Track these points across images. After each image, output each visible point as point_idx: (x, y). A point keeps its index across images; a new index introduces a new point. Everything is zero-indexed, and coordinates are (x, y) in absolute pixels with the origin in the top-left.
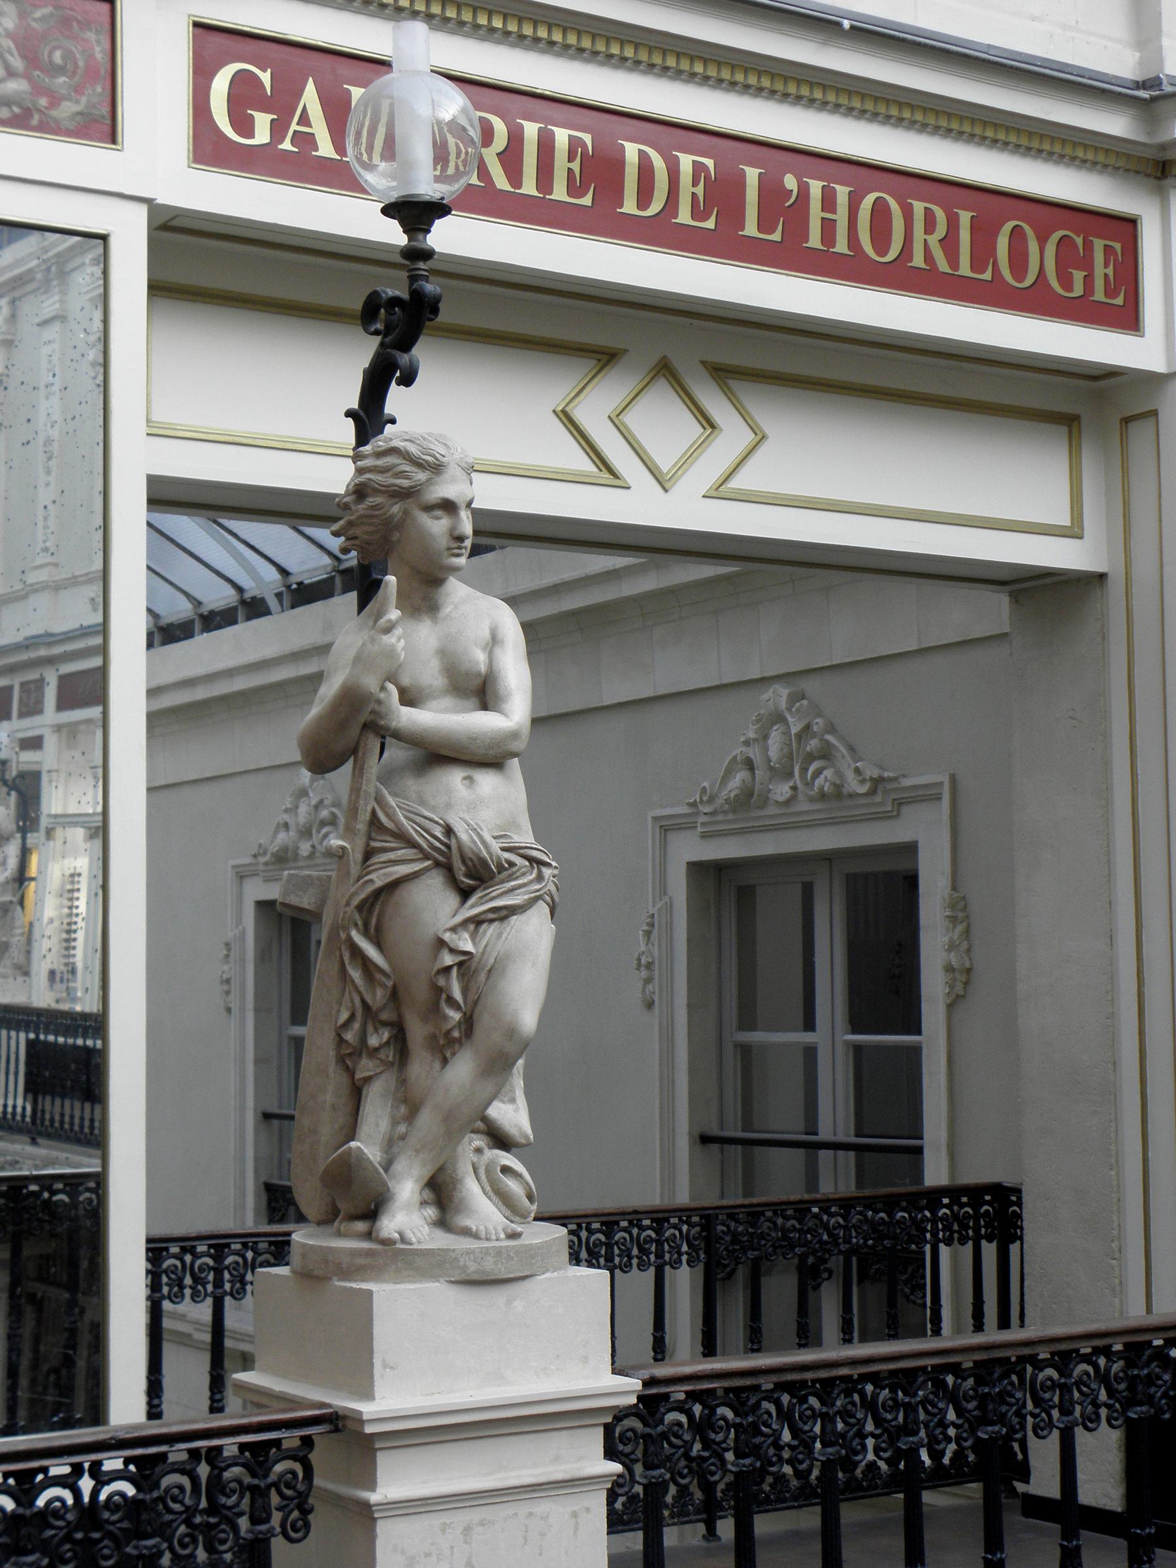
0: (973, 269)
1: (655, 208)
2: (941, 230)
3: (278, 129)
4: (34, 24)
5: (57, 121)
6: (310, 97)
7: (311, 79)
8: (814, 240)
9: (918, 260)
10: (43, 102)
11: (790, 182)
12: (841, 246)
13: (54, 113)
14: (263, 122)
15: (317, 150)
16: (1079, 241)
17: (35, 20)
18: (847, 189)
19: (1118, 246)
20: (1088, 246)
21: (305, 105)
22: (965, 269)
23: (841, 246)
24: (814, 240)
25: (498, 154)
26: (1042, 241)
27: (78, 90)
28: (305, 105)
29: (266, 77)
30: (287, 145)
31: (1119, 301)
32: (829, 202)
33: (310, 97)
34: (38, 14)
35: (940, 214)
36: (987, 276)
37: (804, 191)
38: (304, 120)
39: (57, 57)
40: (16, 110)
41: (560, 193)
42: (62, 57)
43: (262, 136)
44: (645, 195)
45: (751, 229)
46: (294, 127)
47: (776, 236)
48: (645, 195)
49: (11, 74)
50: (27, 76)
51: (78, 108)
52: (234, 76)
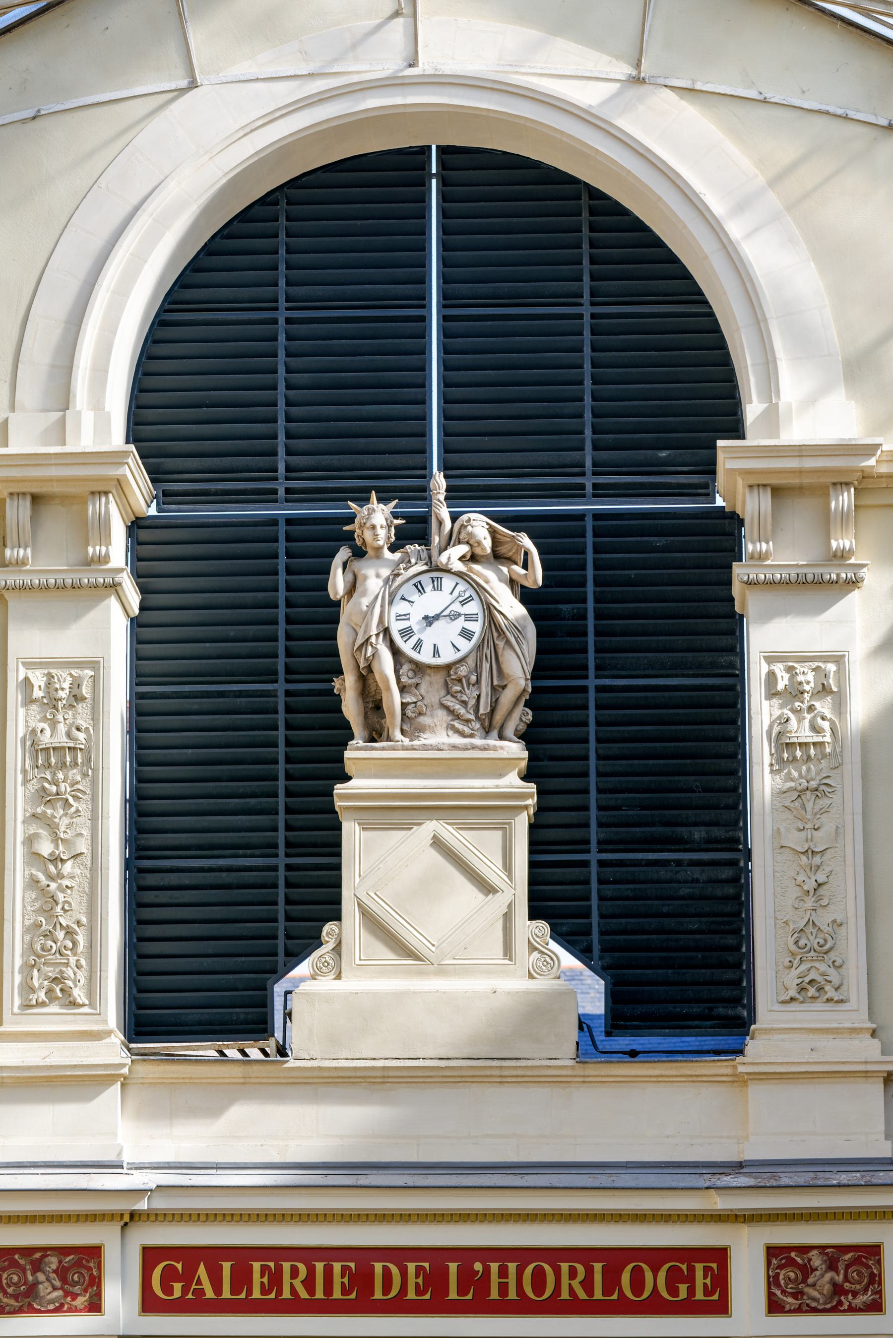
0: (604, 1295)
1: (393, 1294)
2: (581, 1275)
3: (185, 1290)
4: (65, 1264)
5: (76, 1307)
6: (202, 1271)
7: (202, 1263)
8: (494, 1294)
9: (565, 1295)
10: (69, 1299)
11: (478, 1266)
12: (512, 1295)
13: (74, 1303)
14: (178, 1287)
15: (205, 1295)
16: (684, 1267)
17: (66, 1263)
18: (515, 1264)
19: (714, 1266)
20: (691, 1270)
21: (199, 1276)
22: (598, 1295)
23: (512, 1295)
24: (494, 1294)
25: (301, 1282)
26: (655, 1272)
27: (85, 1291)
28: (199, 1276)
29: (179, 1266)
30: (190, 1296)
31: (716, 1297)
32: (503, 1273)
33: (202, 1271)
34: (67, 1260)
35: (580, 1268)
36: (615, 1297)
37: (487, 1270)
38: (199, 1282)
39: (76, 1277)
40: (57, 1304)
41: (337, 1294)
42: (78, 1277)
43: (177, 1293)
44: (387, 1289)
45: (453, 1295)
46: (194, 1287)
47: (470, 1296)
48: (387, 1289)
49: (55, 1288)
50: (62, 1288)
51: (85, 1299)
52: (163, 1268)
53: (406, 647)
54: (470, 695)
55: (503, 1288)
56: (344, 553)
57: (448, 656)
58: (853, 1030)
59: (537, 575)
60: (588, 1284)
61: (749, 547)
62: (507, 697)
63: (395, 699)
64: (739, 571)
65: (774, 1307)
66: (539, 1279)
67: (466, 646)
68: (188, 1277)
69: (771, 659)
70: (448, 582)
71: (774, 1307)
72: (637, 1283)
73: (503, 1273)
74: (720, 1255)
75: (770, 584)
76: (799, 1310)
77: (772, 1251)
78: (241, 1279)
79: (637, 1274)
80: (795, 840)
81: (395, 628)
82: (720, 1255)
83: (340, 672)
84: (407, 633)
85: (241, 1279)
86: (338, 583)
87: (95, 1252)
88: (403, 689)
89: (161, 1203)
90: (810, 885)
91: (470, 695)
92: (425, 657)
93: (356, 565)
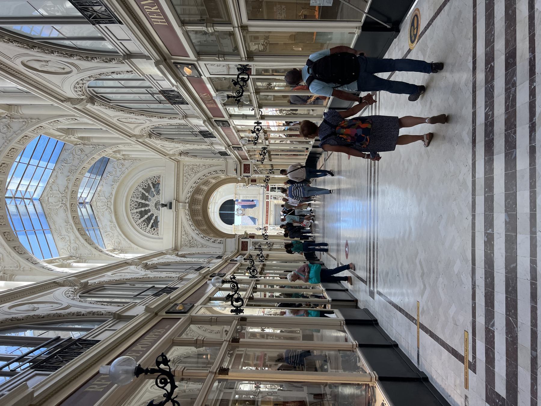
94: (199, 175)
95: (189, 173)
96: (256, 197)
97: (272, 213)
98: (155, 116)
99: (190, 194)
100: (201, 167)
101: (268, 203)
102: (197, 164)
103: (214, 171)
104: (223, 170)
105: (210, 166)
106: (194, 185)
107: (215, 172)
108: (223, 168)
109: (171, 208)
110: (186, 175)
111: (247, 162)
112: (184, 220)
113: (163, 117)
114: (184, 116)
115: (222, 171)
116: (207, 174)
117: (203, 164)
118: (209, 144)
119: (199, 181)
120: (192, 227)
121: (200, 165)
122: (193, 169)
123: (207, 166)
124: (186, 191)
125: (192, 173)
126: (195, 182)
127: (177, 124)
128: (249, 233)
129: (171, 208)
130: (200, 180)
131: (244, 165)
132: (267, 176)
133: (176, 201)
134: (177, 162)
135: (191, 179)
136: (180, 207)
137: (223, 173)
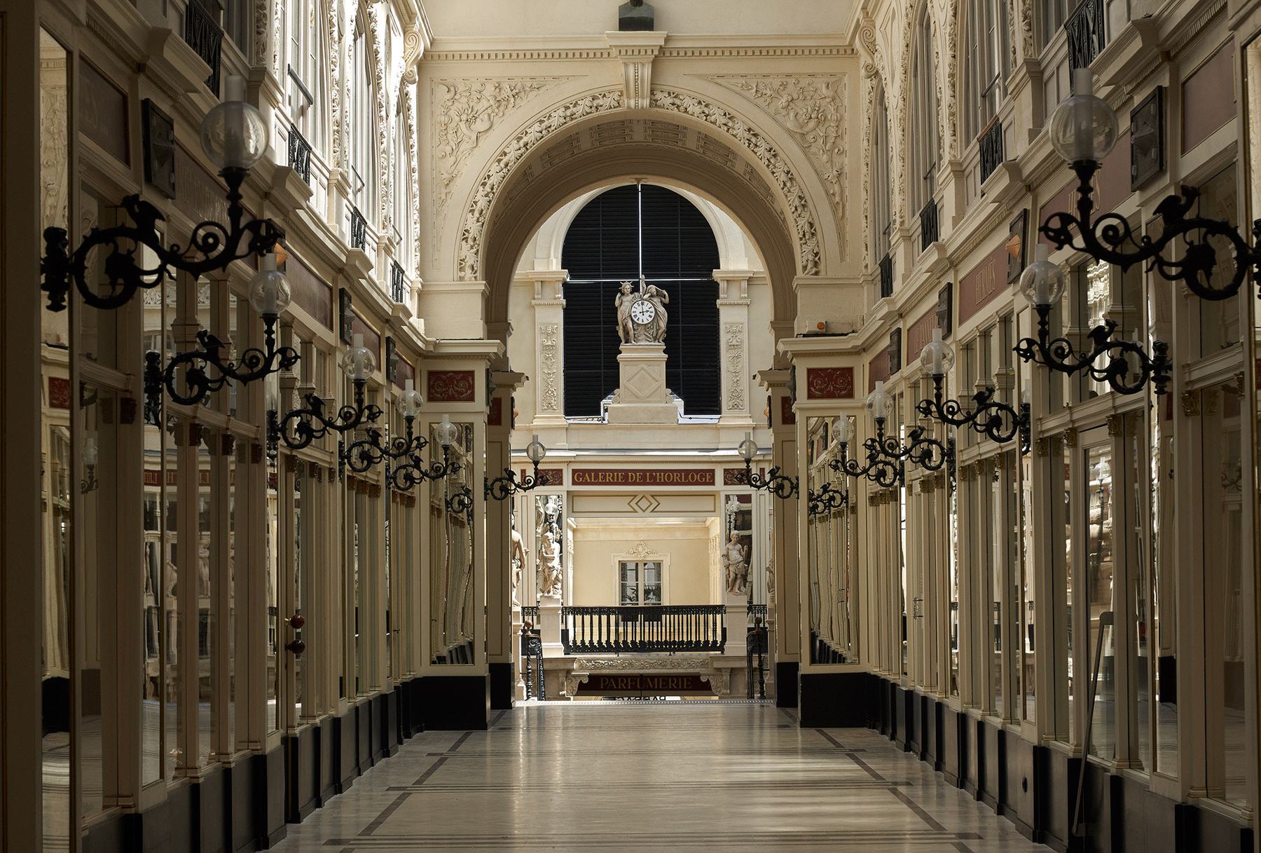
32: (660, 475)
53: (635, 320)
54: (651, 332)
55: (660, 479)
56: (619, 295)
57: (646, 322)
58: (746, 417)
59: (667, 300)
60: (681, 478)
61: (721, 296)
62: (660, 331)
63: (632, 333)
64: (718, 302)
65: (726, 484)
66: (669, 479)
67: (650, 319)
68: (583, 476)
69: (726, 324)
70: (646, 303)
71: (726, 484)
72: (693, 478)
73: (660, 475)
74: (713, 471)
75: (726, 305)
76: (731, 484)
77: (725, 470)
78: (596, 477)
79: (693, 476)
80: (731, 369)
81: (633, 314)
82: (713, 471)
83: (618, 325)
84: (635, 316)
85: (596, 477)
86: (617, 303)
87: (561, 470)
88: (634, 330)
89: (577, 459)
90: (735, 380)
91: (651, 332)
92: (640, 322)
93: (622, 298)
94: (791, 151)
95: (799, 103)
96: (735, 406)
97: (644, 504)
98: (954, 57)
99: (697, 110)
100: (831, 161)
101: (706, 477)
102: (846, 138)
103: (811, 225)
104: (822, 267)
105: (838, 208)
106: (740, 130)
107: (807, 228)
108: (831, 268)
109: (626, 24)
110: (791, 87)
111: (861, 380)
112: (569, 90)
113: (954, 86)
114: (961, 164)
115: (816, 264)
116: (796, 191)
117: (846, 169)
118: (906, 225)
119: (761, 151)
120: (537, 127)
121: (841, 153)
122: (821, 121)
123: (837, 188)
124: (711, 91)
125: (802, 118)
126: (755, 135)
127: (941, 128)
128: (519, 394)
129: (626, 24)
130: (767, 155)
131: (849, 371)
132: (797, 487)
133: (661, 47)
134: (851, 44)
135: (772, 113)
136: (631, 70)
137: (805, 268)
